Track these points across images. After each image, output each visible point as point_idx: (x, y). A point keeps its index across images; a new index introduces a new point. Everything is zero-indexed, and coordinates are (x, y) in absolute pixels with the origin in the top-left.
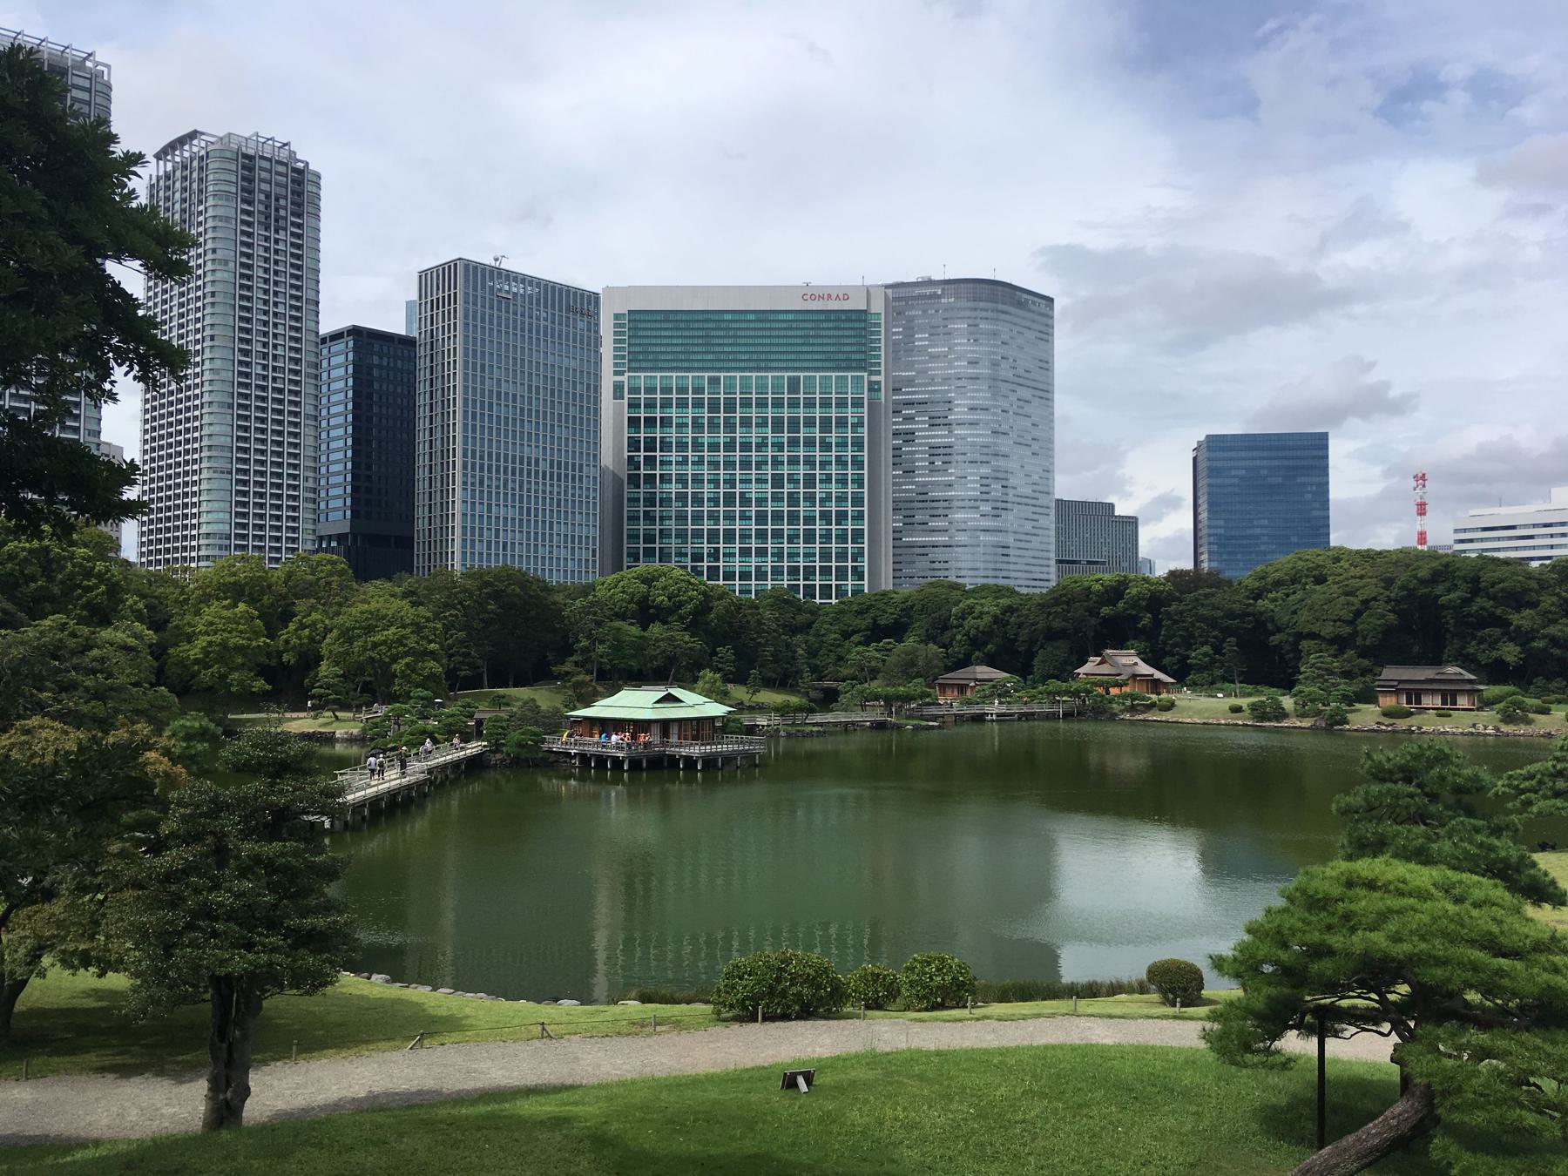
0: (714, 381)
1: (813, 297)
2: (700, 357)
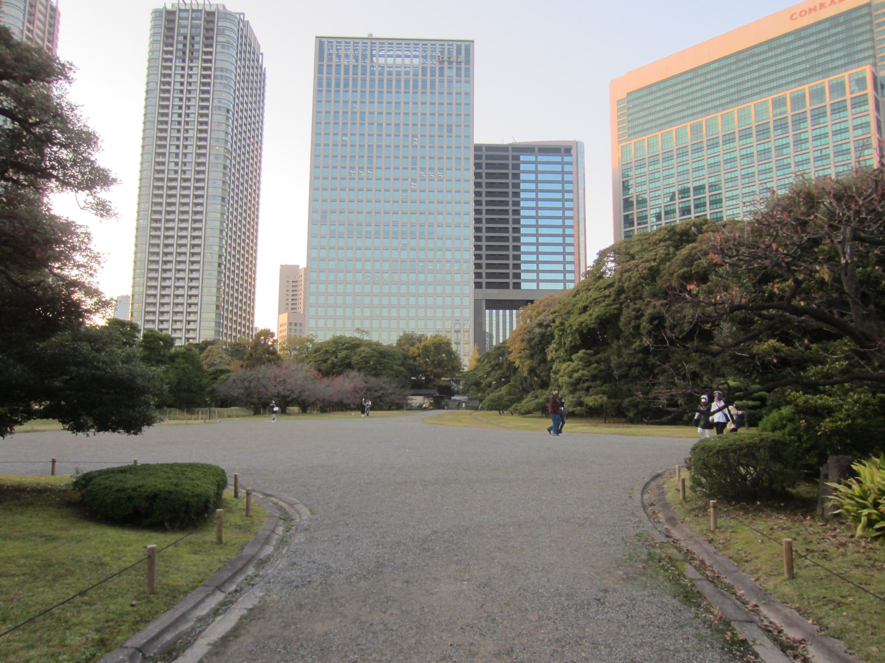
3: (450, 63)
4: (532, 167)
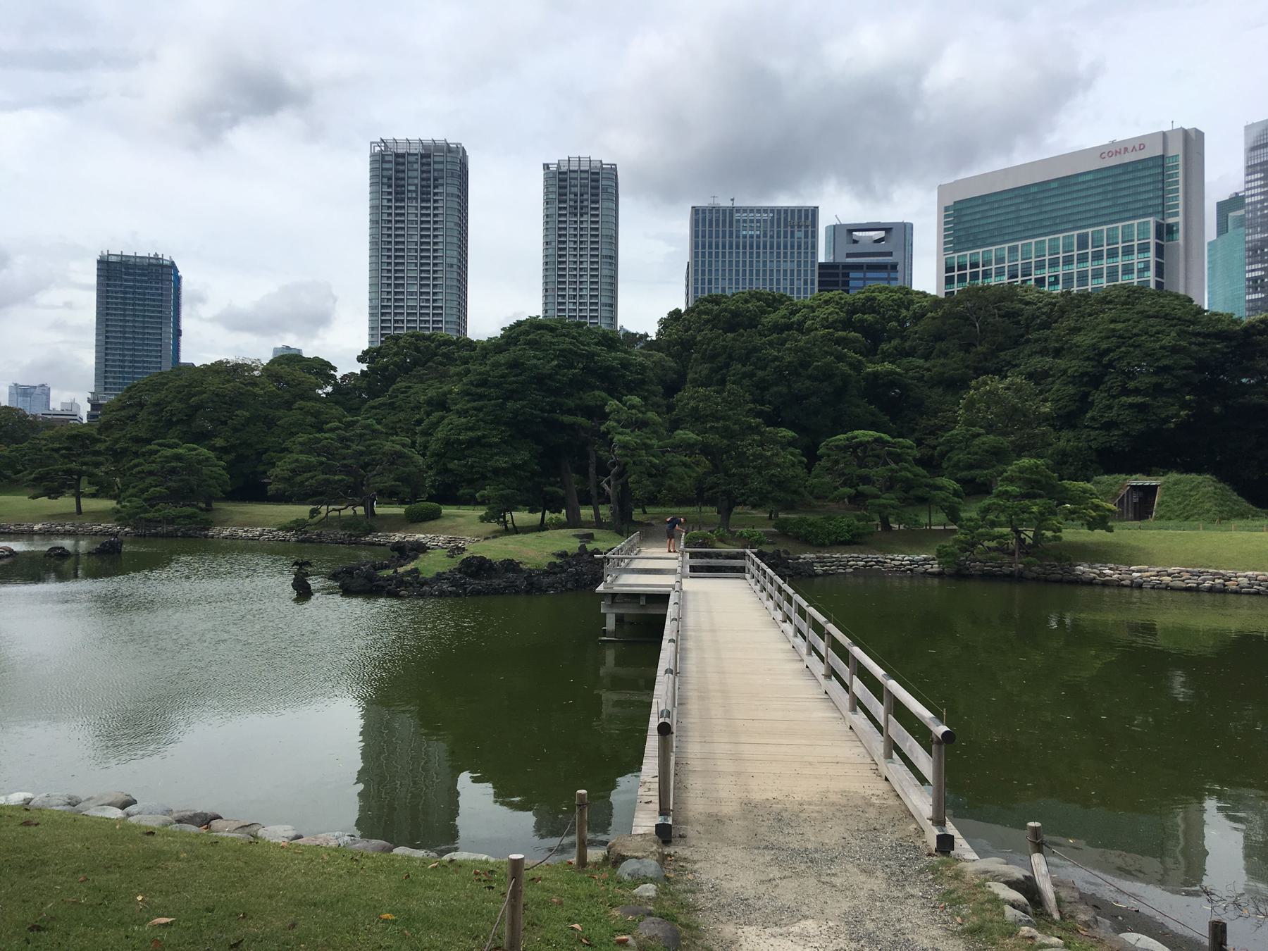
0: (1013, 250)
1: (1111, 154)
2: (1010, 230)
3: (799, 226)
4: (860, 283)
